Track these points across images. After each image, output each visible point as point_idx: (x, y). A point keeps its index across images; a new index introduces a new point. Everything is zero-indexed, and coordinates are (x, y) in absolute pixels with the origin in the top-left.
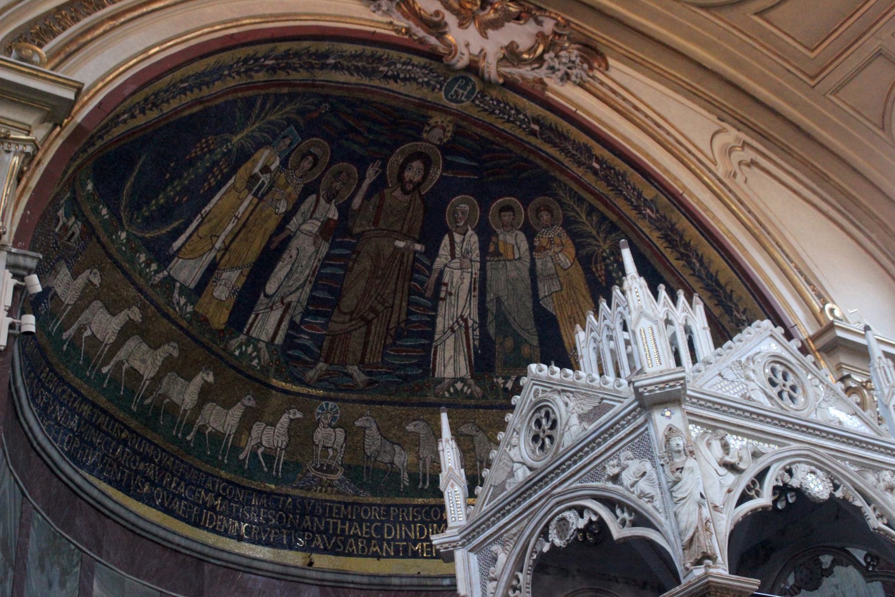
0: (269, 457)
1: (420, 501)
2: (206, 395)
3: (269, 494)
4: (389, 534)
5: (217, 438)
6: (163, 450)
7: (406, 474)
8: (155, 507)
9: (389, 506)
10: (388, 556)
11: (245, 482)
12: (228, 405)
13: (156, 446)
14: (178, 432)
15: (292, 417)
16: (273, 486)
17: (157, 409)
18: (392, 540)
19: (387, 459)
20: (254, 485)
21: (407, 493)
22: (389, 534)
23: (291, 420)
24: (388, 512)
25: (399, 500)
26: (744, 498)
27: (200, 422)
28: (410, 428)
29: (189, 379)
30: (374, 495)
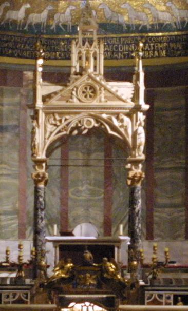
0: (65, 26)
1: (133, 35)
2: (27, 12)
3: (68, 39)
4: (121, 49)
5: (38, 25)
6: (14, 36)
7: (125, 25)
8: (15, 57)
9: (120, 39)
10: (121, 58)
11: (55, 37)
12: (40, 12)
13: (11, 36)
14: (19, 27)
15: (71, 9)
16: (69, 36)
17: (7, 24)
18: (123, 51)
19: (116, 19)
20: (60, 37)
21: (126, 32)
22: (121, 49)
23: (71, 10)
24: (120, 40)
25: (124, 35)
26: (59, 132)
27: (28, 22)
28: (123, 6)
29: (18, 9)
30: (113, 34)
